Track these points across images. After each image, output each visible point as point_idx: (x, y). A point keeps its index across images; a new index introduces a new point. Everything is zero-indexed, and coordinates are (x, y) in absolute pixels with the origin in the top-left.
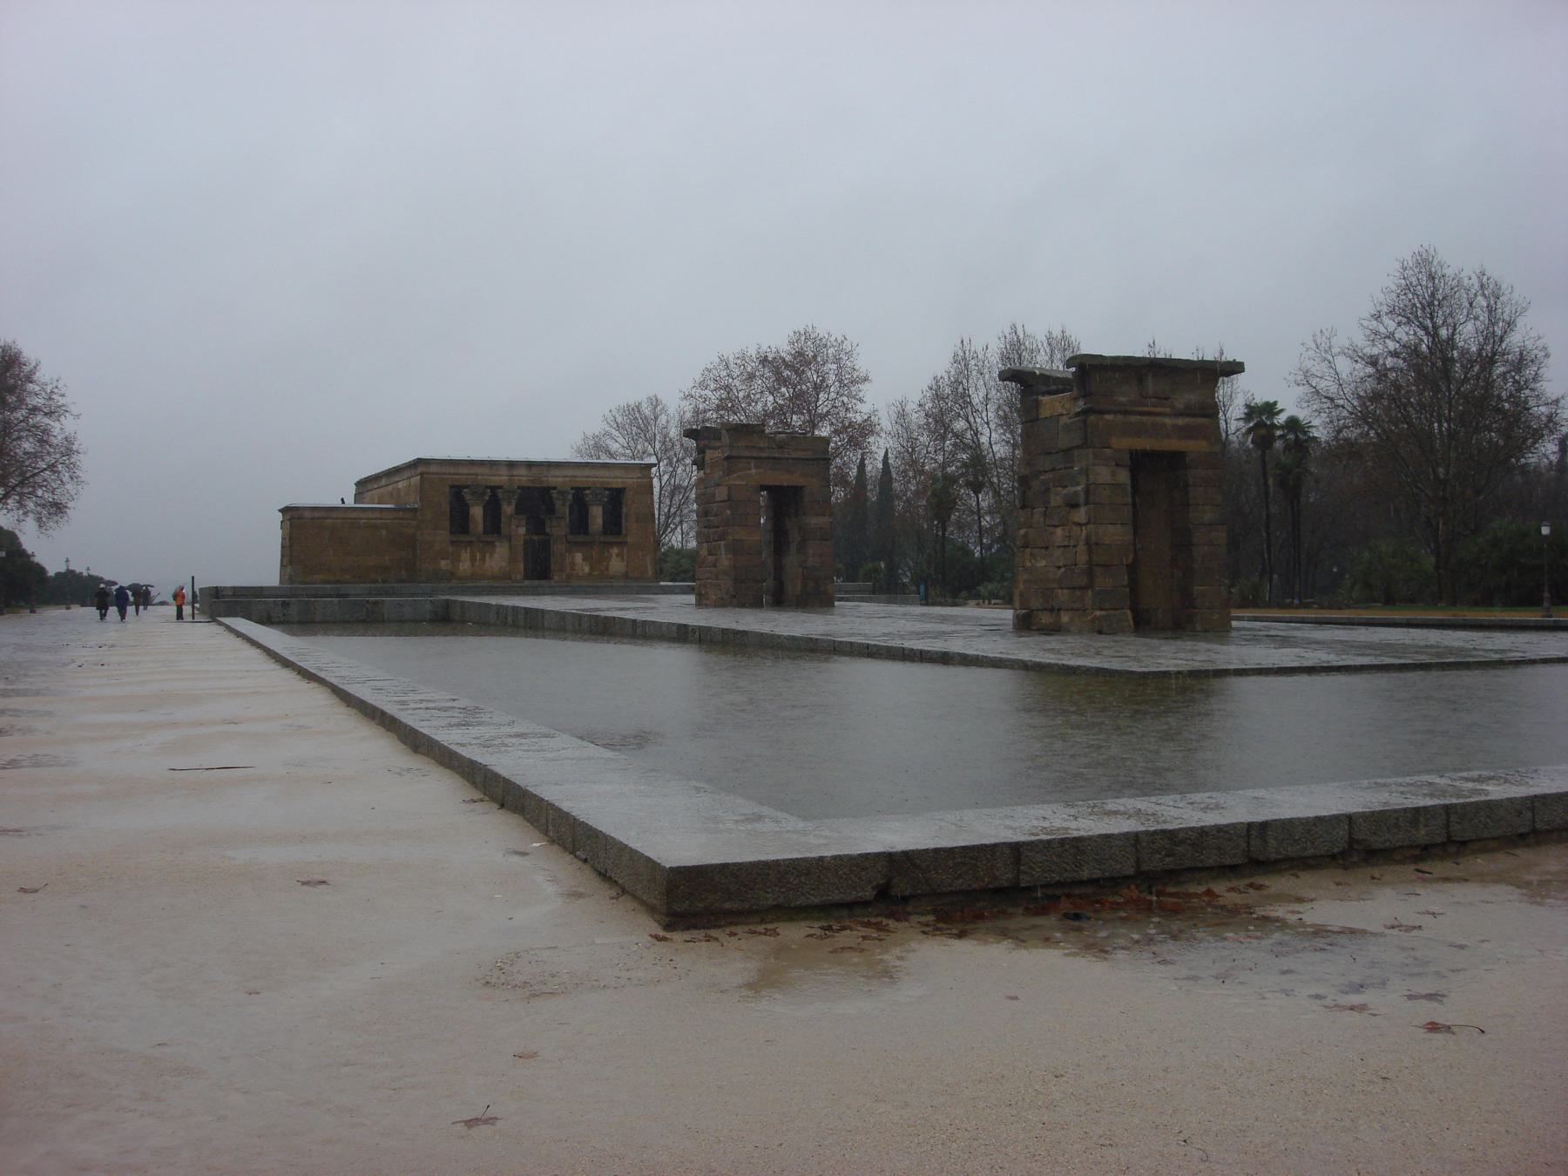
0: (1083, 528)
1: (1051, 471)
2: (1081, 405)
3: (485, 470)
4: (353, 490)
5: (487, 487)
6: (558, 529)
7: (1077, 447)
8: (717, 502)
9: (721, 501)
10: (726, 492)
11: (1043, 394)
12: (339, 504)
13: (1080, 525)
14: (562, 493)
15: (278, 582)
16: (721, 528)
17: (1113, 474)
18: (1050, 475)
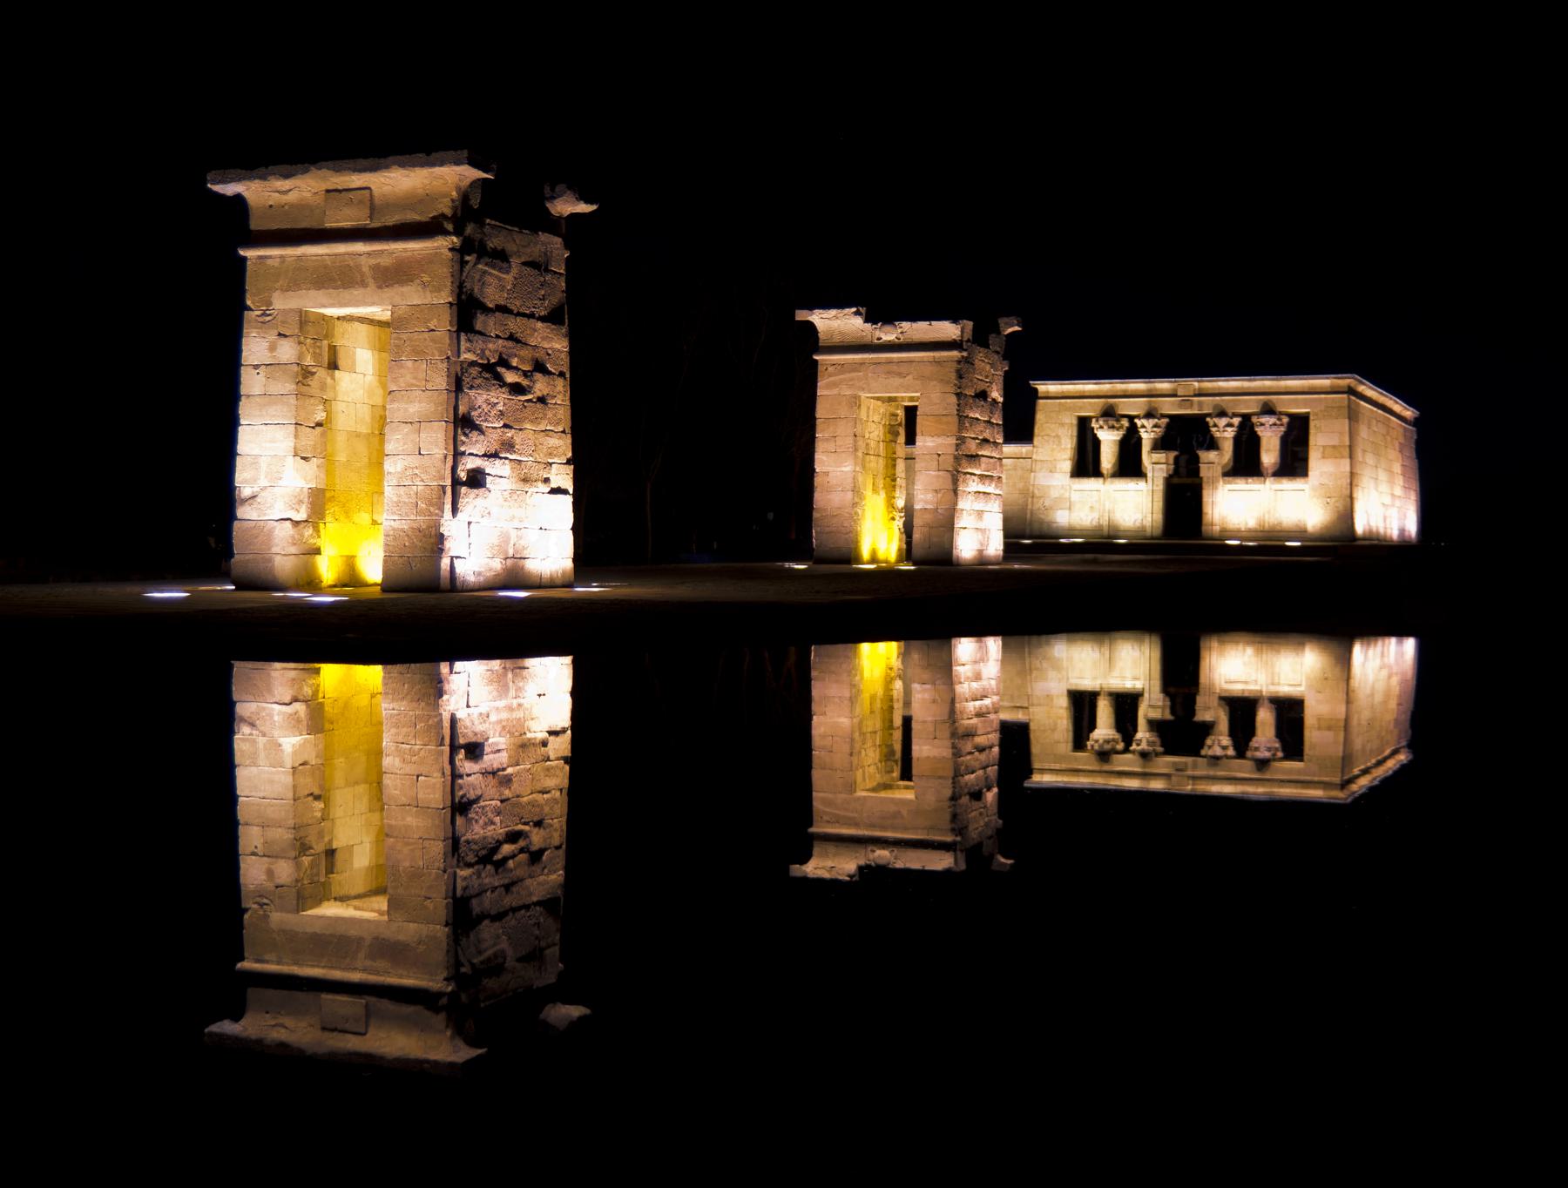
17: (272, 348)
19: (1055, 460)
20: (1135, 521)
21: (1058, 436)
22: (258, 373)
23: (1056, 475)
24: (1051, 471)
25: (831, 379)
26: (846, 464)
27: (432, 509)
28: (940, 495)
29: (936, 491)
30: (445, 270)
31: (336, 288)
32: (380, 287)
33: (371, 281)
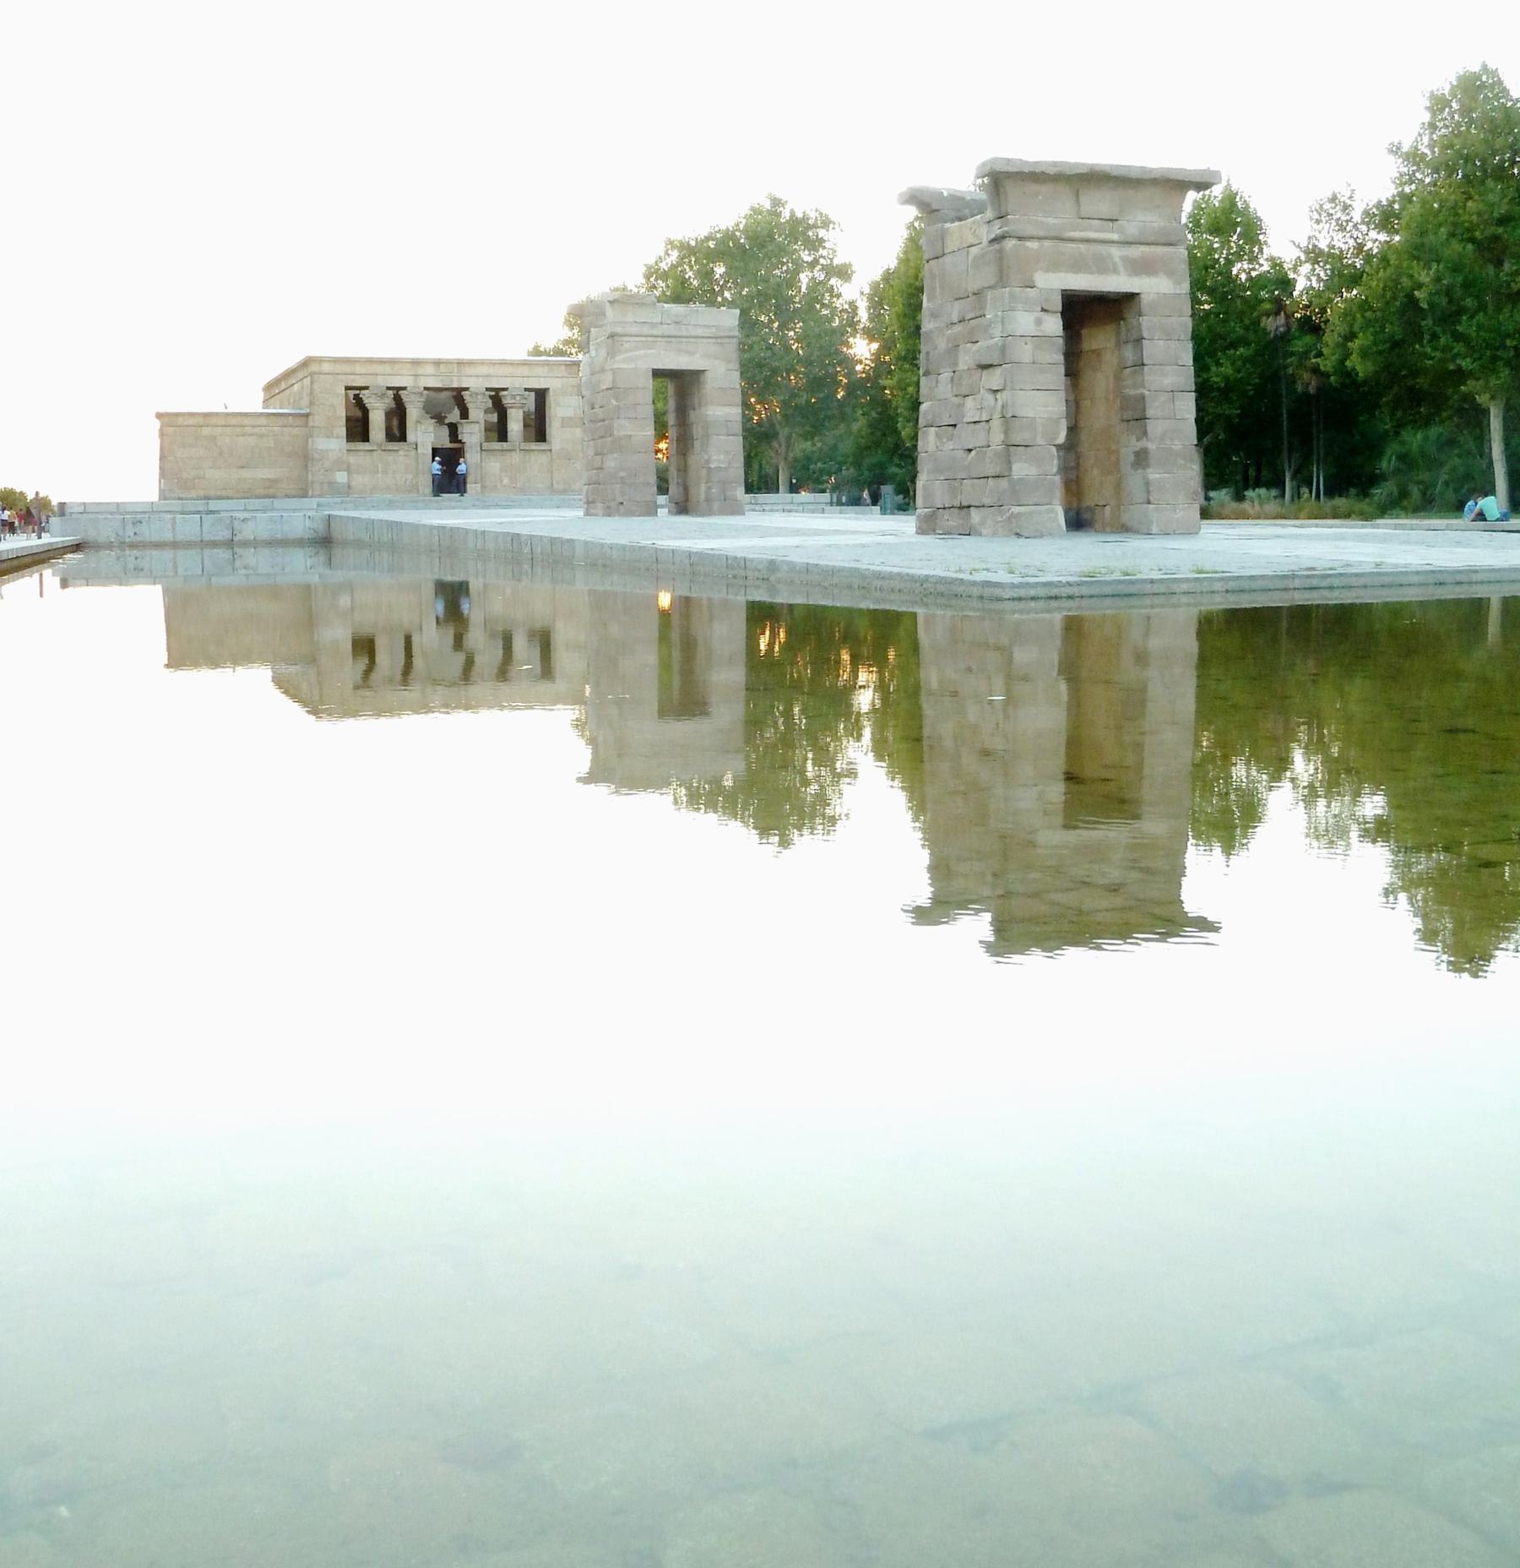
0: (998, 397)
1: (960, 322)
2: (997, 230)
3: (387, 369)
4: (261, 396)
5: (389, 388)
6: (472, 434)
7: (989, 287)
8: (603, 390)
9: (608, 389)
10: (611, 378)
11: (952, 221)
12: (223, 410)
13: (996, 391)
14: (477, 394)
15: (157, 497)
16: (607, 422)
17: (1039, 322)
18: (958, 328)
19: (332, 427)
20: (405, 482)
21: (332, 405)
22: (1026, 344)
23: (334, 440)
24: (328, 437)
25: (629, 354)
26: (647, 429)
27: (1189, 465)
28: (730, 457)
29: (727, 453)
30: (1183, 266)
31: (1091, 273)
32: (1130, 275)
33: (1121, 268)
